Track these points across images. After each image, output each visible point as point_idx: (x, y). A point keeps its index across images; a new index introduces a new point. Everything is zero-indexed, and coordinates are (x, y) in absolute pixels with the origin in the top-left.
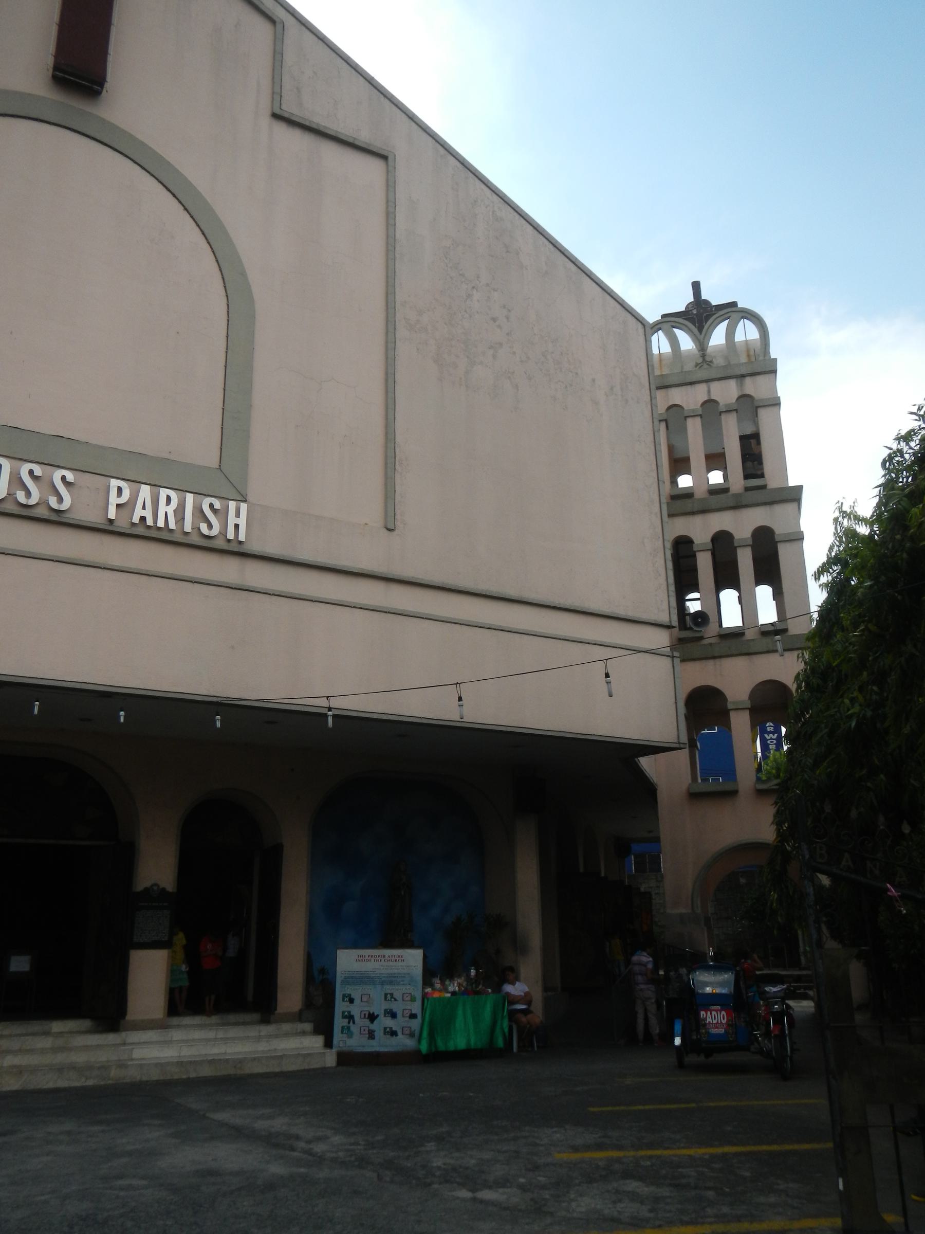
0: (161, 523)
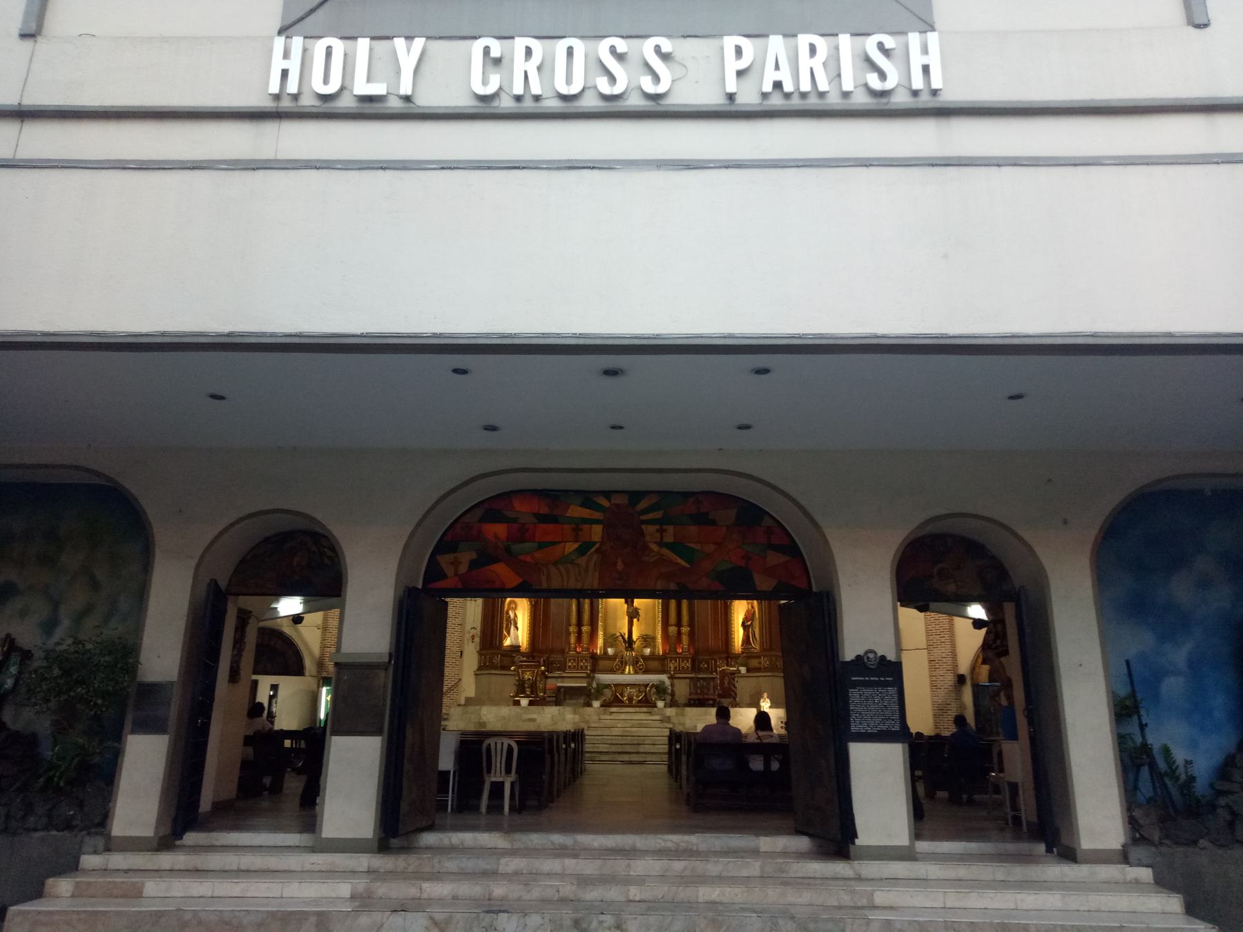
0: (806, 86)
